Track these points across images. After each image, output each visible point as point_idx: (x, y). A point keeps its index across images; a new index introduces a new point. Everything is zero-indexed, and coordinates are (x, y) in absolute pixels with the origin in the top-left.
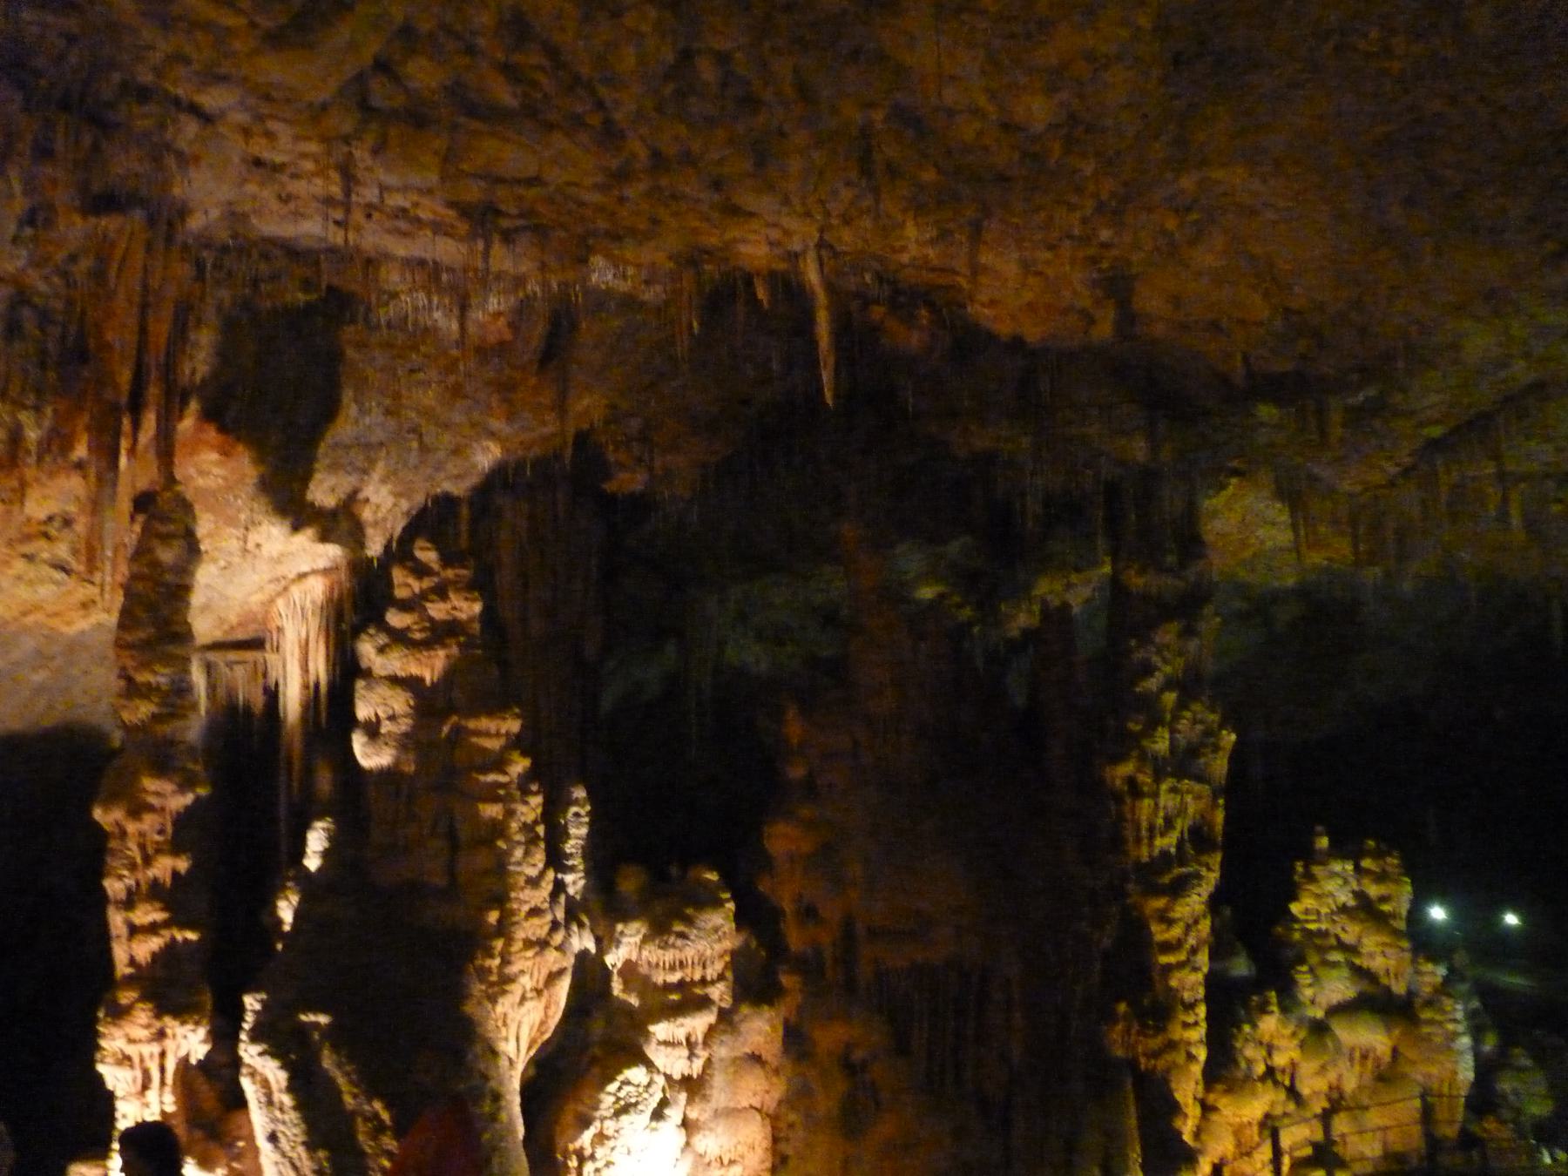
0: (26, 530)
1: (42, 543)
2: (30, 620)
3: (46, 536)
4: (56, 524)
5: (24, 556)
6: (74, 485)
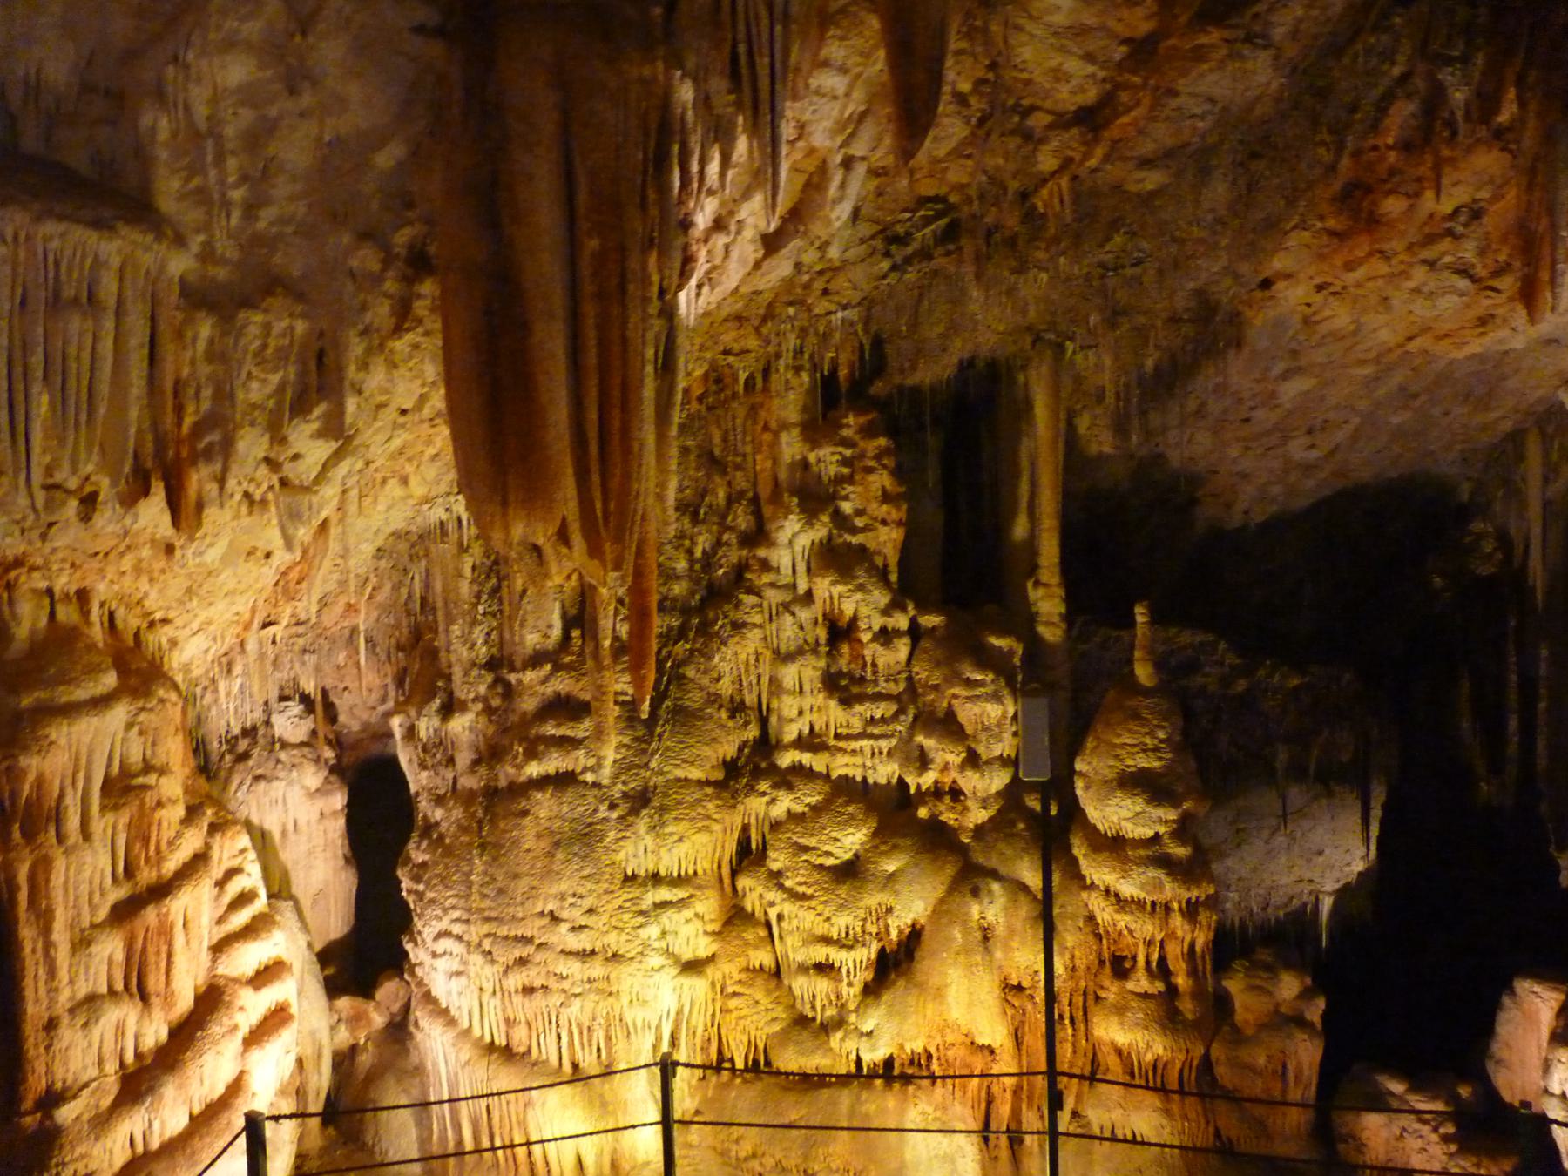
0: (1427, 230)
1: (1446, 244)
2: (1412, 346)
3: (1450, 233)
4: (1462, 219)
5: (1424, 262)
6: (1489, 161)
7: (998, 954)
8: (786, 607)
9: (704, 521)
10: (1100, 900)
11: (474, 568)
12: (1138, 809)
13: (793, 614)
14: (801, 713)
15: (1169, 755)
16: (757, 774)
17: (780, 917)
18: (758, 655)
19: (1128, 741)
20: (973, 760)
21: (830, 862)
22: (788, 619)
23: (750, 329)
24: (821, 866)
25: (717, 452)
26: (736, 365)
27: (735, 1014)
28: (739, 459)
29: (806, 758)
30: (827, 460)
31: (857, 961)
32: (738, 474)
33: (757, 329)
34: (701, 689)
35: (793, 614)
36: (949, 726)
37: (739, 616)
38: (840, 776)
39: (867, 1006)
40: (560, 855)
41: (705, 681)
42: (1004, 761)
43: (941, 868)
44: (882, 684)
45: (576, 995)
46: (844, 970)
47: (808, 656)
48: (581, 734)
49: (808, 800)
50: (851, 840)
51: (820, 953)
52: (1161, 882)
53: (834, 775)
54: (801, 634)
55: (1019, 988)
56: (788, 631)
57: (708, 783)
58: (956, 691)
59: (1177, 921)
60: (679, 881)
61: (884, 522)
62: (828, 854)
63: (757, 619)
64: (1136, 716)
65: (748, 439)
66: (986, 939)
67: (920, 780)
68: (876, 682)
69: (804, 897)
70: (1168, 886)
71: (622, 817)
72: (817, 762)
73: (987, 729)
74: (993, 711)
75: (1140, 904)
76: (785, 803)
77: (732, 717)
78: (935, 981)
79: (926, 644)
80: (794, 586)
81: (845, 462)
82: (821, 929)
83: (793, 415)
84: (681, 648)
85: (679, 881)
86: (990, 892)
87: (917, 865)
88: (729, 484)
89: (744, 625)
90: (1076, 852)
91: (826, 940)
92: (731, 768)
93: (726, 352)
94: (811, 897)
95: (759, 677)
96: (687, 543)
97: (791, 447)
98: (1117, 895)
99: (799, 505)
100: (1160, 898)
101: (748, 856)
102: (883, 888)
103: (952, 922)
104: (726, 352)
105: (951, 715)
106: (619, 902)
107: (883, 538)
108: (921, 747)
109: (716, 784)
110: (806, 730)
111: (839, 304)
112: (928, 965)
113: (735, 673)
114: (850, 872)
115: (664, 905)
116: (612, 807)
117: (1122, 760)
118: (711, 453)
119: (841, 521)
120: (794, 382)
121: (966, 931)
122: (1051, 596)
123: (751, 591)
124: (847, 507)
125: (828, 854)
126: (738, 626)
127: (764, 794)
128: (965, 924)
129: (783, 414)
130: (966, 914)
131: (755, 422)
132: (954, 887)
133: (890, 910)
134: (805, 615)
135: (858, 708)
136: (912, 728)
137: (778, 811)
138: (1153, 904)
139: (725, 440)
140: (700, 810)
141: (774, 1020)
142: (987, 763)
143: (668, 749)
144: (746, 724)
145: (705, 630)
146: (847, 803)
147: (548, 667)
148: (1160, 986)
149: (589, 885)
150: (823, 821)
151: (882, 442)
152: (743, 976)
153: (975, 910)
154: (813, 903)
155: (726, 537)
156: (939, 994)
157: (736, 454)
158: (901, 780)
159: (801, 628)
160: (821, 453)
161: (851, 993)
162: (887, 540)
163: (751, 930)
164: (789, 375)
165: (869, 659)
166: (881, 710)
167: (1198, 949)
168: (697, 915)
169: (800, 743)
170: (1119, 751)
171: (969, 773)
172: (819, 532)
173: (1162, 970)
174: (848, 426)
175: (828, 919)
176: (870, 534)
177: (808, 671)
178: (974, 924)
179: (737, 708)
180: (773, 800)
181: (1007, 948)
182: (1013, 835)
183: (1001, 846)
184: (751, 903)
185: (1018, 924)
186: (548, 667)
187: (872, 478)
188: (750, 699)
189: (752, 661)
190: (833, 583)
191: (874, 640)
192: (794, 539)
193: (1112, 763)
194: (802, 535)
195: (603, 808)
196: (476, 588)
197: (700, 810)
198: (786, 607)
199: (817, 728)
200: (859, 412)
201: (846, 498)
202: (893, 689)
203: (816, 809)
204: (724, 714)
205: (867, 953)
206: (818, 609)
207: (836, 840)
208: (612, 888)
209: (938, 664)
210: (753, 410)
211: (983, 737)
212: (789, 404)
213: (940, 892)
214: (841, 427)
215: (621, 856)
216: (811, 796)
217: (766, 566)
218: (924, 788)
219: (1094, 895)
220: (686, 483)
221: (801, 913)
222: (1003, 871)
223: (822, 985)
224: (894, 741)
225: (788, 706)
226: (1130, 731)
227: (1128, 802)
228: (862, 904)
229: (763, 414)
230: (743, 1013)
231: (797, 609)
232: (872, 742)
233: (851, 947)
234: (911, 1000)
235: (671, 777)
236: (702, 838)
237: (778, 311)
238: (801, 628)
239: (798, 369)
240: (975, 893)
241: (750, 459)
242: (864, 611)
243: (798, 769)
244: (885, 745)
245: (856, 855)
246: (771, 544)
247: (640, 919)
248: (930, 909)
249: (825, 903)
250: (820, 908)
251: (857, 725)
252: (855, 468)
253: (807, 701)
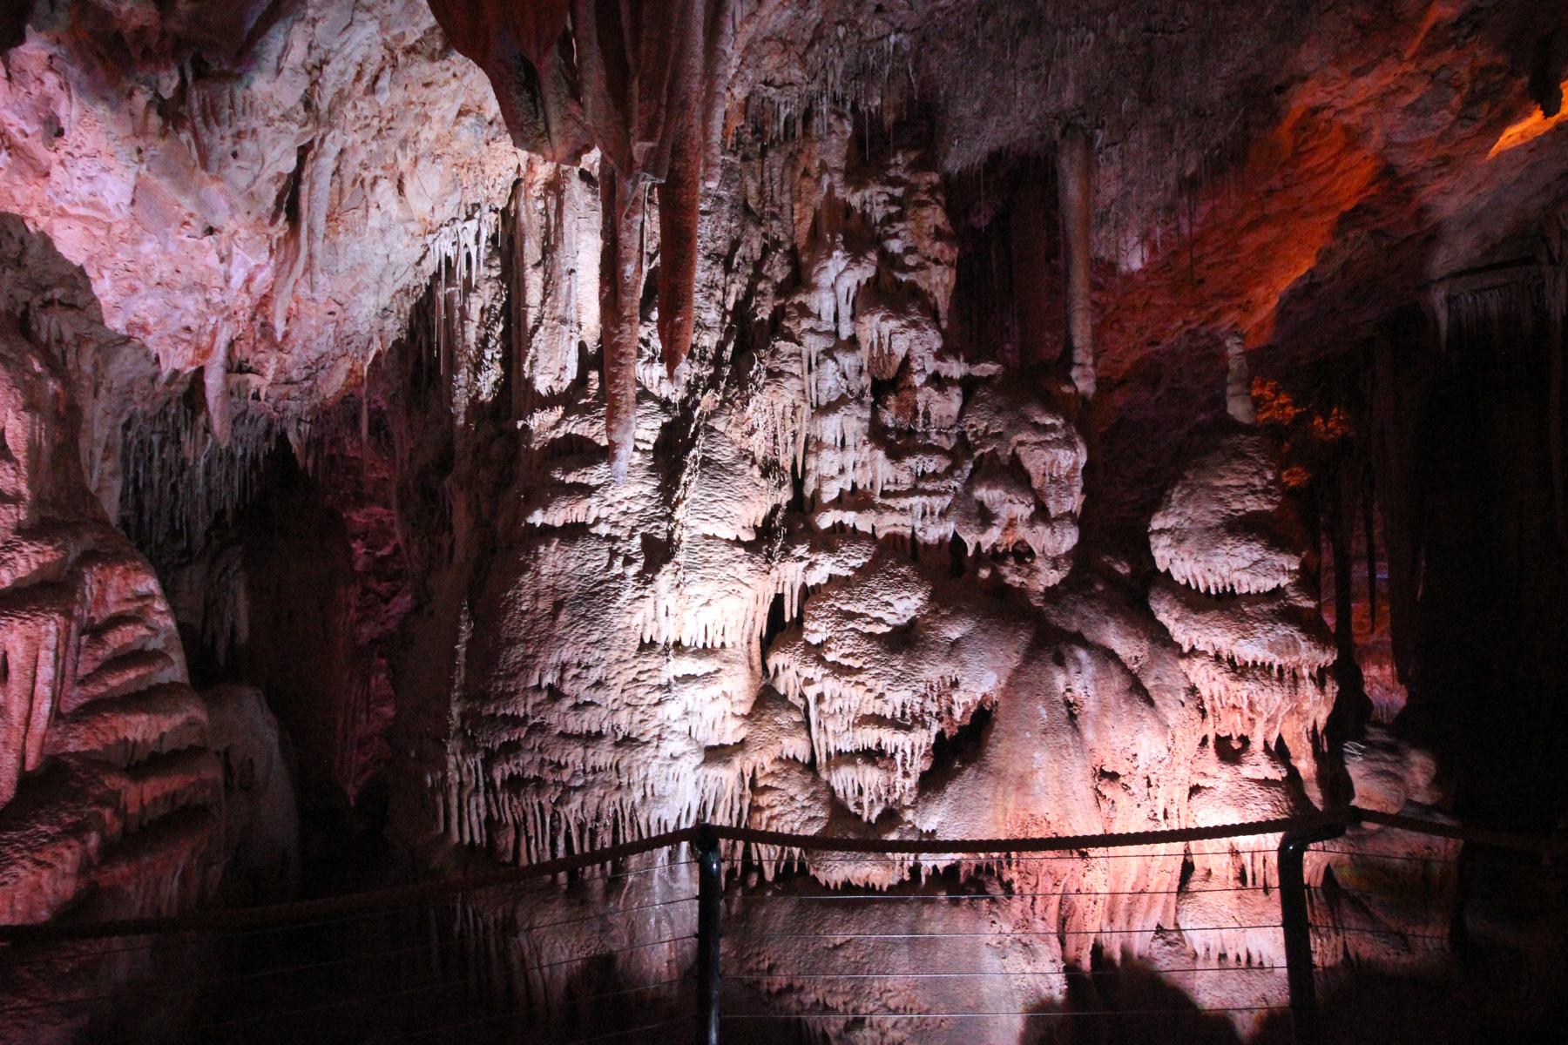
7: (1089, 735)
8: (828, 353)
9: (736, 271)
10: (1210, 667)
11: (482, 310)
12: (1256, 556)
13: (835, 360)
14: (842, 471)
15: (1278, 499)
16: (792, 540)
17: (820, 698)
18: (795, 408)
19: (1231, 482)
20: (1041, 514)
22: (831, 364)
23: (793, 56)
24: (871, 636)
25: (751, 204)
26: (777, 99)
27: (767, 813)
28: (776, 210)
29: (849, 518)
30: (872, 199)
31: (914, 745)
32: (775, 223)
33: (802, 58)
34: (732, 443)
35: (835, 360)
36: (1014, 475)
37: (776, 365)
38: (888, 535)
39: (927, 800)
40: (563, 618)
41: (736, 435)
43: (1014, 634)
44: (934, 436)
45: (576, 789)
46: (899, 758)
47: (852, 405)
48: (594, 482)
49: (853, 563)
50: (905, 605)
51: (869, 737)
52: (1295, 640)
53: (881, 535)
54: (844, 383)
55: (1114, 776)
56: (830, 380)
57: (738, 542)
58: (1022, 437)
59: (1309, 689)
60: (705, 652)
61: (937, 262)
62: (880, 620)
63: (795, 368)
64: (1240, 455)
65: (786, 187)
66: (1072, 717)
67: (982, 539)
68: (927, 435)
69: (850, 671)
70: (1303, 645)
71: (639, 575)
73: (1056, 481)
75: (1266, 669)
76: (826, 568)
77: (765, 475)
78: (1017, 767)
79: (982, 393)
80: (837, 333)
81: (893, 200)
82: (873, 707)
83: (836, 161)
85: (705, 652)
86: (1077, 661)
87: (985, 631)
88: (765, 235)
89: (781, 373)
90: (1162, 617)
91: (878, 720)
94: (860, 670)
95: (795, 435)
96: (719, 294)
98: (1231, 661)
99: (844, 242)
100: (1288, 661)
101: (780, 629)
102: (948, 657)
103: (1034, 695)
105: (1015, 459)
106: (632, 674)
107: (936, 279)
108: (981, 503)
110: (849, 488)
111: (892, 24)
112: (1000, 751)
113: (771, 428)
114: (904, 641)
115: (687, 678)
116: (628, 561)
117: (1227, 505)
118: (747, 210)
120: (837, 126)
121: (1051, 705)
122: (1085, 376)
123: (789, 337)
124: (895, 246)
125: (880, 620)
126: (774, 375)
127: (801, 559)
128: (1048, 697)
129: (826, 158)
130: (1051, 685)
131: (794, 168)
132: (1029, 657)
133: (955, 684)
134: (848, 361)
135: (910, 462)
136: (970, 484)
137: (817, 577)
138: (1280, 669)
139: (761, 192)
140: (730, 571)
141: (811, 819)
142: (1056, 519)
143: (694, 501)
144: (780, 485)
146: (900, 564)
147: (560, 410)
148: (1277, 774)
149: (597, 653)
150: (872, 584)
152: (777, 768)
153: (1060, 680)
154: (862, 677)
155: (761, 286)
156: (1022, 783)
157: (774, 205)
158: (957, 543)
159: (844, 376)
160: (867, 194)
161: (905, 785)
162: (939, 282)
163: (785, 714)
164: (832, 118)
165: (921, 407)
166: (932, 464)
167: (1320, 728)
168: (724, 693)
169: (841, 502)
170: (1222, 495)
171: (1040, 528)
172: (865, 272)
173: (1279, 753)
174: (897, 164)
175: (881, 695)
176: (923, 273)
177: (852, 422)
178: (1059, 698)
180: (811, 565)
181: (1098, 727)
182: (1093, 597)
183: (1082, 609)
184: (786, 683)
185: (1112, 700)
186: (560, 410)
187: (926, 212)
188: (785, 461)
189: (789, 415)
190: (883, 319)
191: (926, 384)
192: (838, 278)
193: (1215, 507)
194: (847, 274)
195: (619, 562)
196: (483, 331)
197: (730, 571)
198: (828, 353)
199: (860, 486)
200: (906, 148)
201: (896, 236)
202: (948, 445)
203: (863, 572)
204: (756, 472)
205: (923, 738)
206: (863, 355)
207: (888, 604)
208: (625, 656)
209: (999, 411)
211: (1052, 490)
213: (1015, 661)
214: (889, 167)
215: (638, 619)
217: (804, 311)
218: (985, 548)
219: (1198, 662)
220: (718, 233)
221: (848, 690)
222: (1088, 635)
223: (871, 777)
224: (948, 499)
226: (1234, 471)
227: (1243, 548)
228: (921, 676)
229: (803, 161)
230: (776, 811)
231: (839, 356)
232: (924, 499)
233: (909, 729)
234: (985, 791)
235: (695, 532)
236: (732, 604)
237: (826, 31)
238: (844, 376)
239: (841, 116)
240: (1060, 662)
241: (787, 211)
242: (918, 350)
243: (839, 528)
244: (938, 503)
245: (913, 622)
247: (658, 695)
248: (1004, 681)
249: (876, 676)
250: (870, 683)
251: (906, 480)
252: (903, 208)
253: (850, 457)
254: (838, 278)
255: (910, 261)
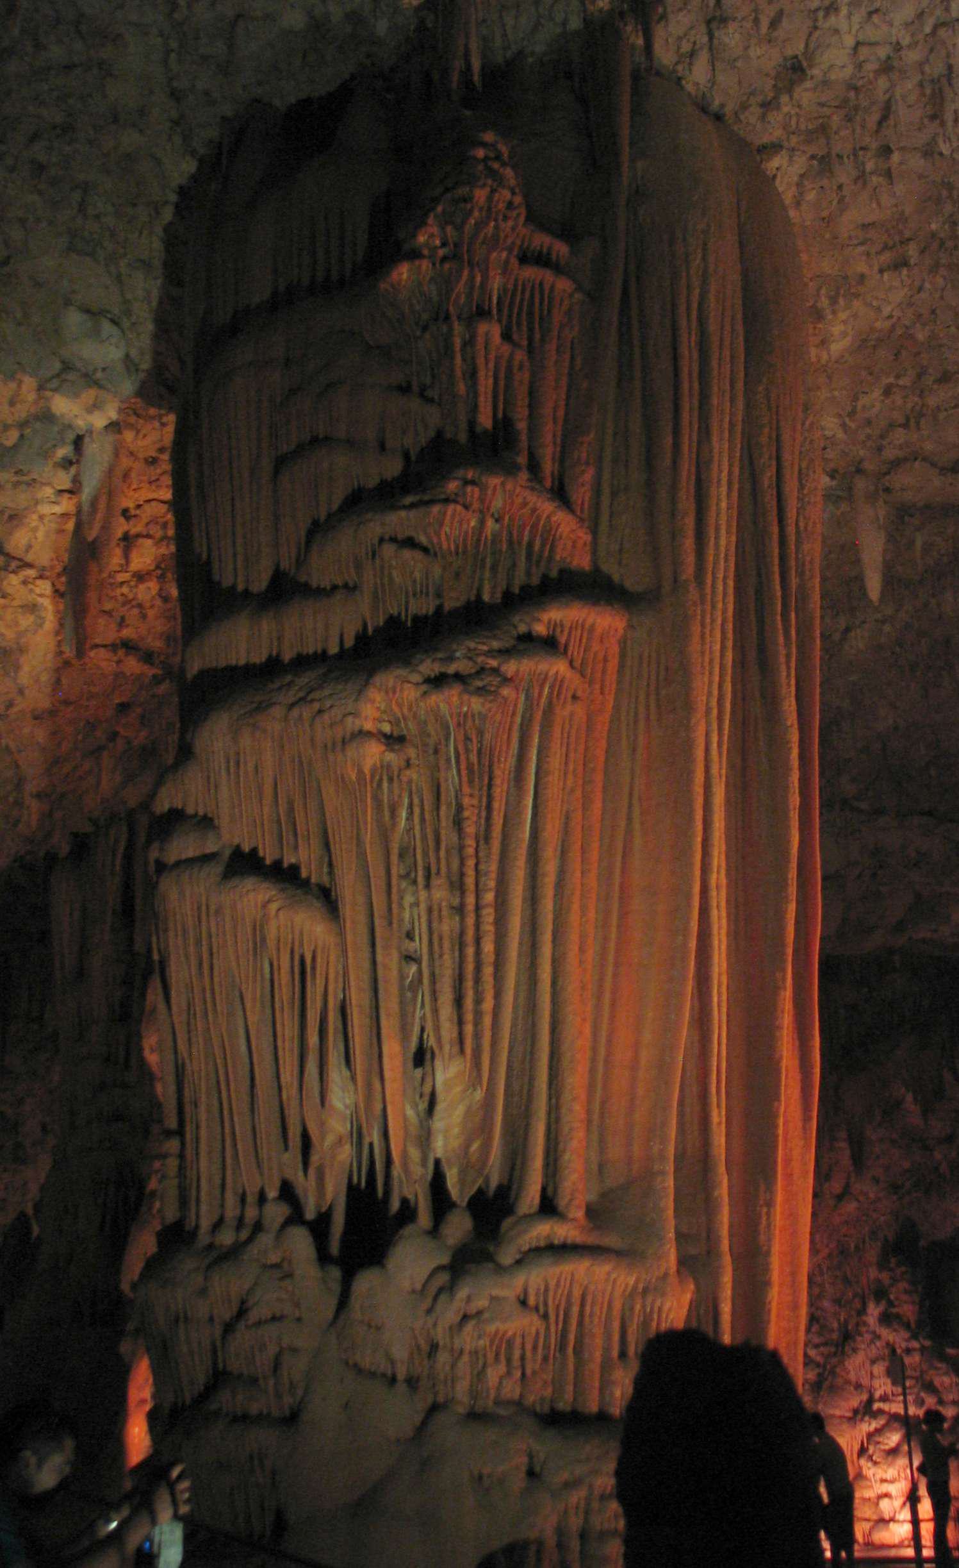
16: (864, 1414)
20: (941, 1402)
21: (887, 1447)
42: (953, 1402)
56: (874, 1352)
72: (885, 1407)
74: (946, 1380)
84: (834, 1360)
92: (856, 1412)
93: (845, 1236)
97: (873, 1273)
104: (845, 1236)
109: (850, 1419)
119: (891, 1304)
126: (855, 1350)
145: (843, 1353)
151: (903, 1269)
179: (858, 1386)
192: (874, 1311)
202: (914, 1374)
203: (884, 1426)
210: (860, 1258)
212: (872, 1254)
216: (882, 1421)
217: (865, 1324)
225: (876, 1383)
242: (897, 1340)
246: (866, 1314)
254: (874, 1311)
255: (896, 1303)
